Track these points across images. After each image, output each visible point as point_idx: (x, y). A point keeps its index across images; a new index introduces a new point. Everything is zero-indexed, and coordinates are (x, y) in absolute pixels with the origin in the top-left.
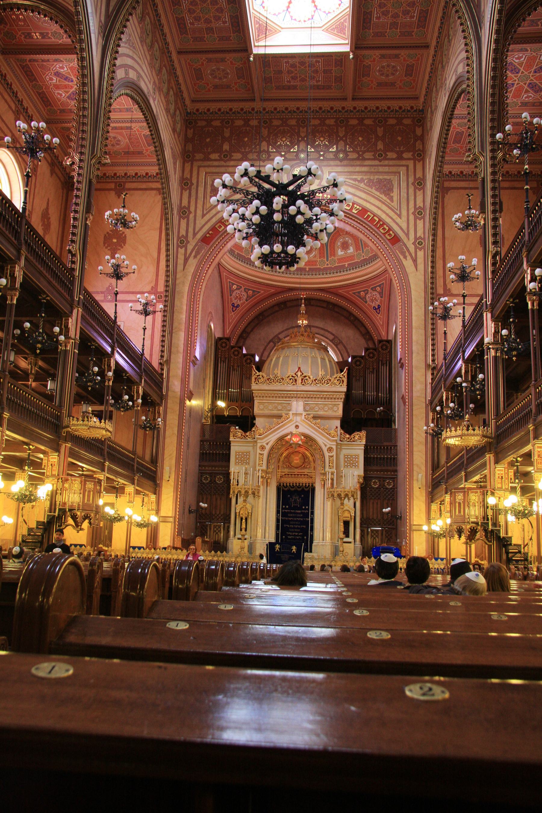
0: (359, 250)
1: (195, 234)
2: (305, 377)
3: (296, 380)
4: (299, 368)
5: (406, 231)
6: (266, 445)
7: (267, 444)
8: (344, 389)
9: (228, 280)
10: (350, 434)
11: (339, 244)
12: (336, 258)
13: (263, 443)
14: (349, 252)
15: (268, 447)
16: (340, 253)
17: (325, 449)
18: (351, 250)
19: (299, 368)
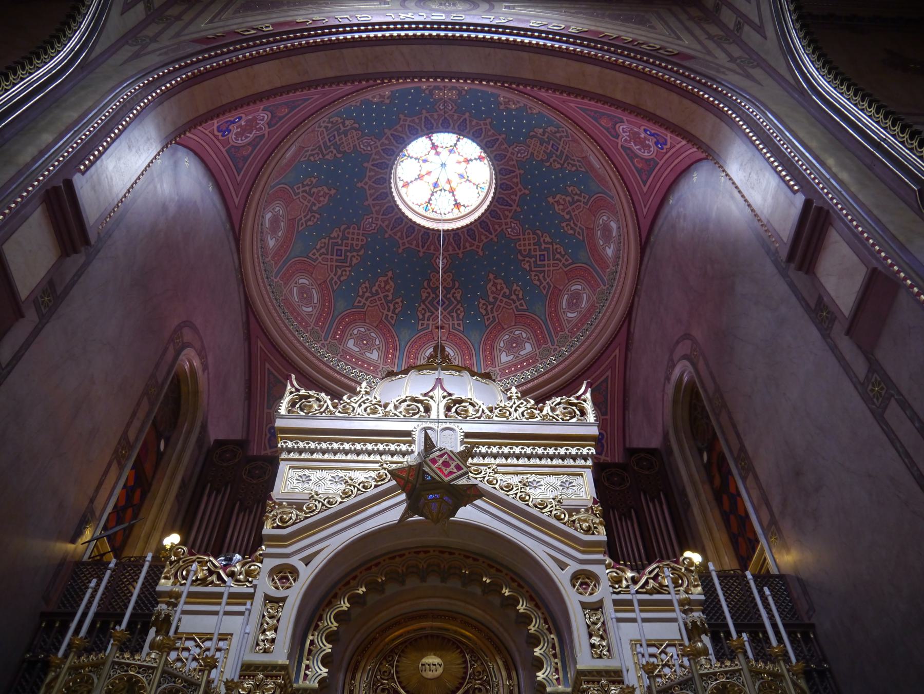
0: (545, 342)
1: (178, 35)
2: (459, 401)
3: (427, 409)
4: (439, 381)
5: (704, 51)
6: (300, 566)
7: (307, 561)
8: (594, 431)
9: (267, 365)
10: (639, 569)
11: (502, 345)
12: (497, 368)
13: (287, 556)
14: (522, 353)
15: (307, 574)
16: (504, 358)
17: (562, 578)
18: (528, 348)
19: (439, 381)
